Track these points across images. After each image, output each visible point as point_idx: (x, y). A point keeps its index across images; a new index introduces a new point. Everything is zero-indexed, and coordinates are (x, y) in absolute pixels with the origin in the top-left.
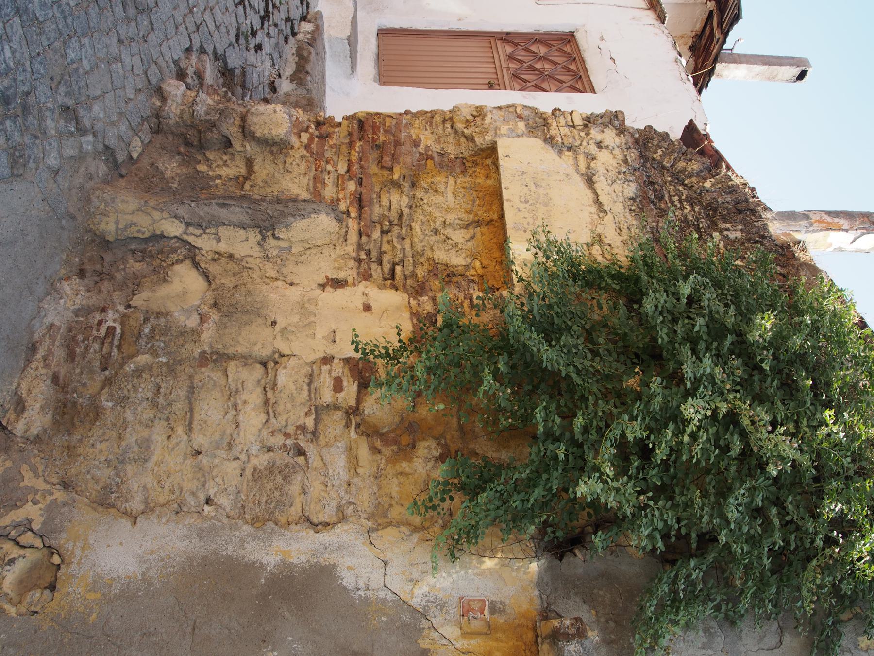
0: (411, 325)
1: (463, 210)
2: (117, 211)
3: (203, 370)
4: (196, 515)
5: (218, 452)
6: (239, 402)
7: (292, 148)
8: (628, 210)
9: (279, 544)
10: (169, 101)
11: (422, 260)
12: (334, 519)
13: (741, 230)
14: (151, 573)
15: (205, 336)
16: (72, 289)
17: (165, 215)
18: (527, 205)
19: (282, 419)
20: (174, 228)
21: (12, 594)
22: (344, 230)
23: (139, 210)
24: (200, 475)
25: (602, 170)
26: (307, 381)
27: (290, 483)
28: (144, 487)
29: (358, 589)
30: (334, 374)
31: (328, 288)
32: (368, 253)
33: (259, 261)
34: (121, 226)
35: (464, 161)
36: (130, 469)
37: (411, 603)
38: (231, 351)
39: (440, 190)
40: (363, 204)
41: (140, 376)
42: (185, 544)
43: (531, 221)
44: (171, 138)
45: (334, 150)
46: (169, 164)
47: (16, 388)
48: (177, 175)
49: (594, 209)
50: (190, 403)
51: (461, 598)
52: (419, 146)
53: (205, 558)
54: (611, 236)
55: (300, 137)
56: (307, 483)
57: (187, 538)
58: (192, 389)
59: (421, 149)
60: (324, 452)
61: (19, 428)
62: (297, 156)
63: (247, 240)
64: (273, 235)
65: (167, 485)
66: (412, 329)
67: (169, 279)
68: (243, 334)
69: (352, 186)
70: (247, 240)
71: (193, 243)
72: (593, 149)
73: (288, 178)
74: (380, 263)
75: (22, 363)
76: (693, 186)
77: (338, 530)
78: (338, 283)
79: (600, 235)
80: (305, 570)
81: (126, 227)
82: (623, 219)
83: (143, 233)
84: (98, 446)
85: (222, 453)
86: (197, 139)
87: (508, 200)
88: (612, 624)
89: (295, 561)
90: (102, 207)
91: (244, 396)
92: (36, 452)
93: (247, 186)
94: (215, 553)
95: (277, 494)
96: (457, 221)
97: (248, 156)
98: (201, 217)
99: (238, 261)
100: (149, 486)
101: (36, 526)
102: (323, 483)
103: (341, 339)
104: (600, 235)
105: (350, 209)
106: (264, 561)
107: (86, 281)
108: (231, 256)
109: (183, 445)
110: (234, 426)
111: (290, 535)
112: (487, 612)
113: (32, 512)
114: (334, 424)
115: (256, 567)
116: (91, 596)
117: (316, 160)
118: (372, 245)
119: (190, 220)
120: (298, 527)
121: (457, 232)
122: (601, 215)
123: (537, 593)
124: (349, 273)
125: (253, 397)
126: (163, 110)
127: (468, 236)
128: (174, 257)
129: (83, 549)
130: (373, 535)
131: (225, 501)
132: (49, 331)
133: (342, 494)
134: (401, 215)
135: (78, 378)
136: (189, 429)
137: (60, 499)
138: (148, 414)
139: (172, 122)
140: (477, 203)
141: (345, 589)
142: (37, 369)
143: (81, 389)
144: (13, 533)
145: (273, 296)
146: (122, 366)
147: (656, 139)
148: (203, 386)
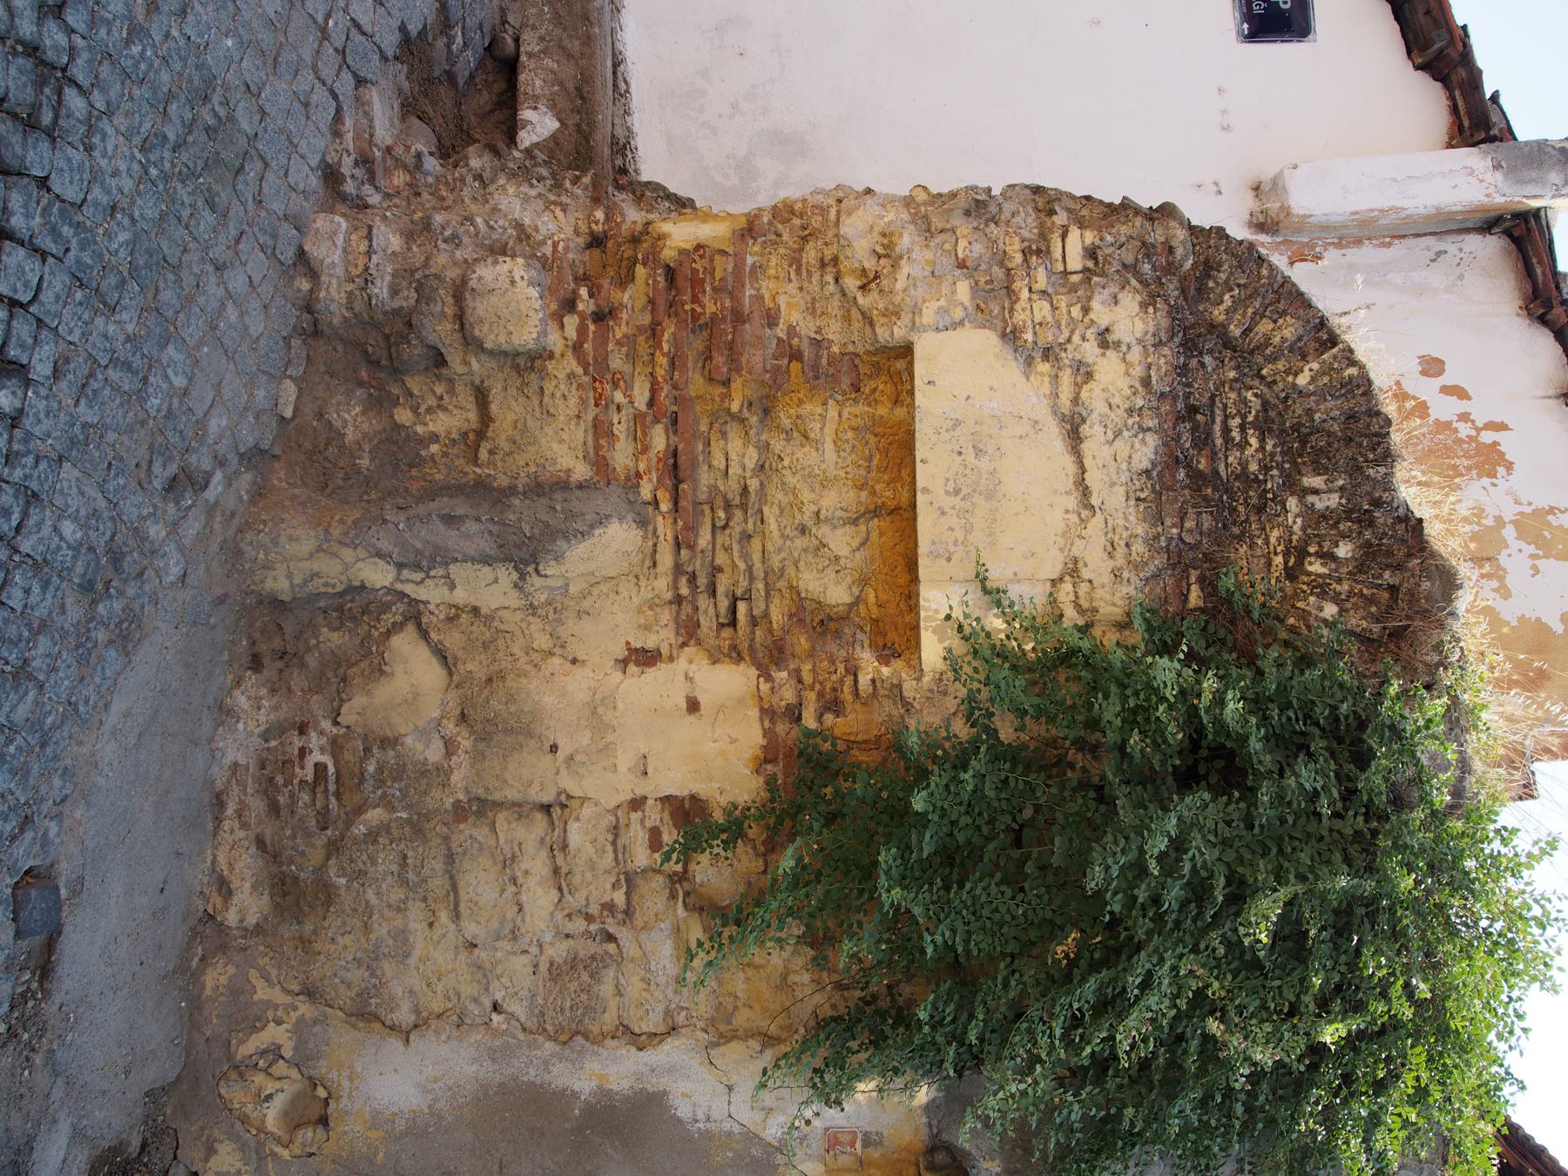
0: (760, 732)
1: (850, 483)
2: (285, 559)
3: (462, 826)
4: (482, 1028)
5: (500, 944)
6: (518, 874)
7: (551, 356)
8: (1132, 502)
9: (593, 1065)
10: (324, 278)
11: (782, 584)
12: (662, 1029)
13: (1342, 489)
14: (439, 1105)
15: (457, 778)
16: (249, 698)
17: (361, 553)
18: (956, 501)
19: (580, 897)
20: (379, 575)
21: (279, 1133)
22: (651, 543)
23: (319, 549)
24: (479, 976)
25: (1099, 406)
26: (610, 838)
27: (599, 981)
28: (411, 992)
29: (696, 1121)
30: (649, 824)
31: (632, 668)
32: (693, 578)
33: (519, 615)
34: (297, 581)
35: (857, 361)
36: (388, 968)
37: (762, 1135)
38: (497, 796)
39: (812, 435)
40: (681, 474)
41: (375, 842)
42: (474, 1068)
43: (959, 534)
44: (340, 348)
45: (624, 349)
46: (349, 412)
47: (213, 863)
48: (365, 435)
49: (1072, 502)
50: (452, 877)
51: (827, 1129)
52: (777, 325)
53: (501, 1085)
54: (1097, 565)
55: (562, 326)
56: (623, 981)
57: (476, 1060)
58: (450, 857)
59: (781, 331)
60: (643, 937)
61: (232, 918)
62: (562, 376)
63: (496, 581)
64: (536, 570)
65: (440, 988)
66: (762, 742)
67: (386, 668)
68: (511, 766)
69: (659, 439)
70: (496, 581)
71: (413, 596)
72: (1090, 350)
73: (549, 430)
74: (713, 593)
75: (210, 826)
76: (1275, 382)
77: (670, 1044)
78: (645, 658)
79: (1076, 561)
80: (627, 1099)
81: (305, 582)
82: (1121, 522)
83: (334, 586)
84: (340, 940)
85: (505, 945)
86: (385, 353)
87: (925, 490)
88: (1019, 1151)
89: (615, 1087)
90: (261, 556)
91: (525, 865)
92: (262, 948)
93: (483, 455)
94: (515, 1079)
95: (584, 997)
96: (839, 513)
97: (477, 382)
98: (418, 552)
99: (489, 619)
100: (416, 989)
101: (287, 1053)
102: (642, 980)
103: (656, 769)
104: (1076, 561)
105: (660, 495)
106: (576, 1088)
107: (266, 673)
108: (475, 611)
109: (451, 936)
110: (516, 909)
111: (605, 1053)
112: (858, 1145)
113: (275, 1034)
114: (653, 897)
115: (564, 1097)
116: (373, 1134)
117: (595, 380)
118: (698, 563)
119: (401, 559)
120: (614, 1043)
121: (839, 532)
122: (1085, 513)
123: (924, 1120)
124: (662, 637)
125: (536, 865)
126: (317, 300)
127: (856, 543)
128: (389, 619)
129: (351, 1079)
130: (712, 1052)
131: (516, 1008)
132: (234, 774)
133: (671, 995)
134: (745, 490)
135: (290, 843)
136: (457, 916)
137: (308, 1015)
138: (397, 894)
139: (336, 321)
140: (875, 462)
141: (679, 1120)
142: (232, 831)
143: (298, 859)
144: (261, 1063)
145: (549, 700)
146: (349, 824)
147: (1226, 267)
148: (464, 853)
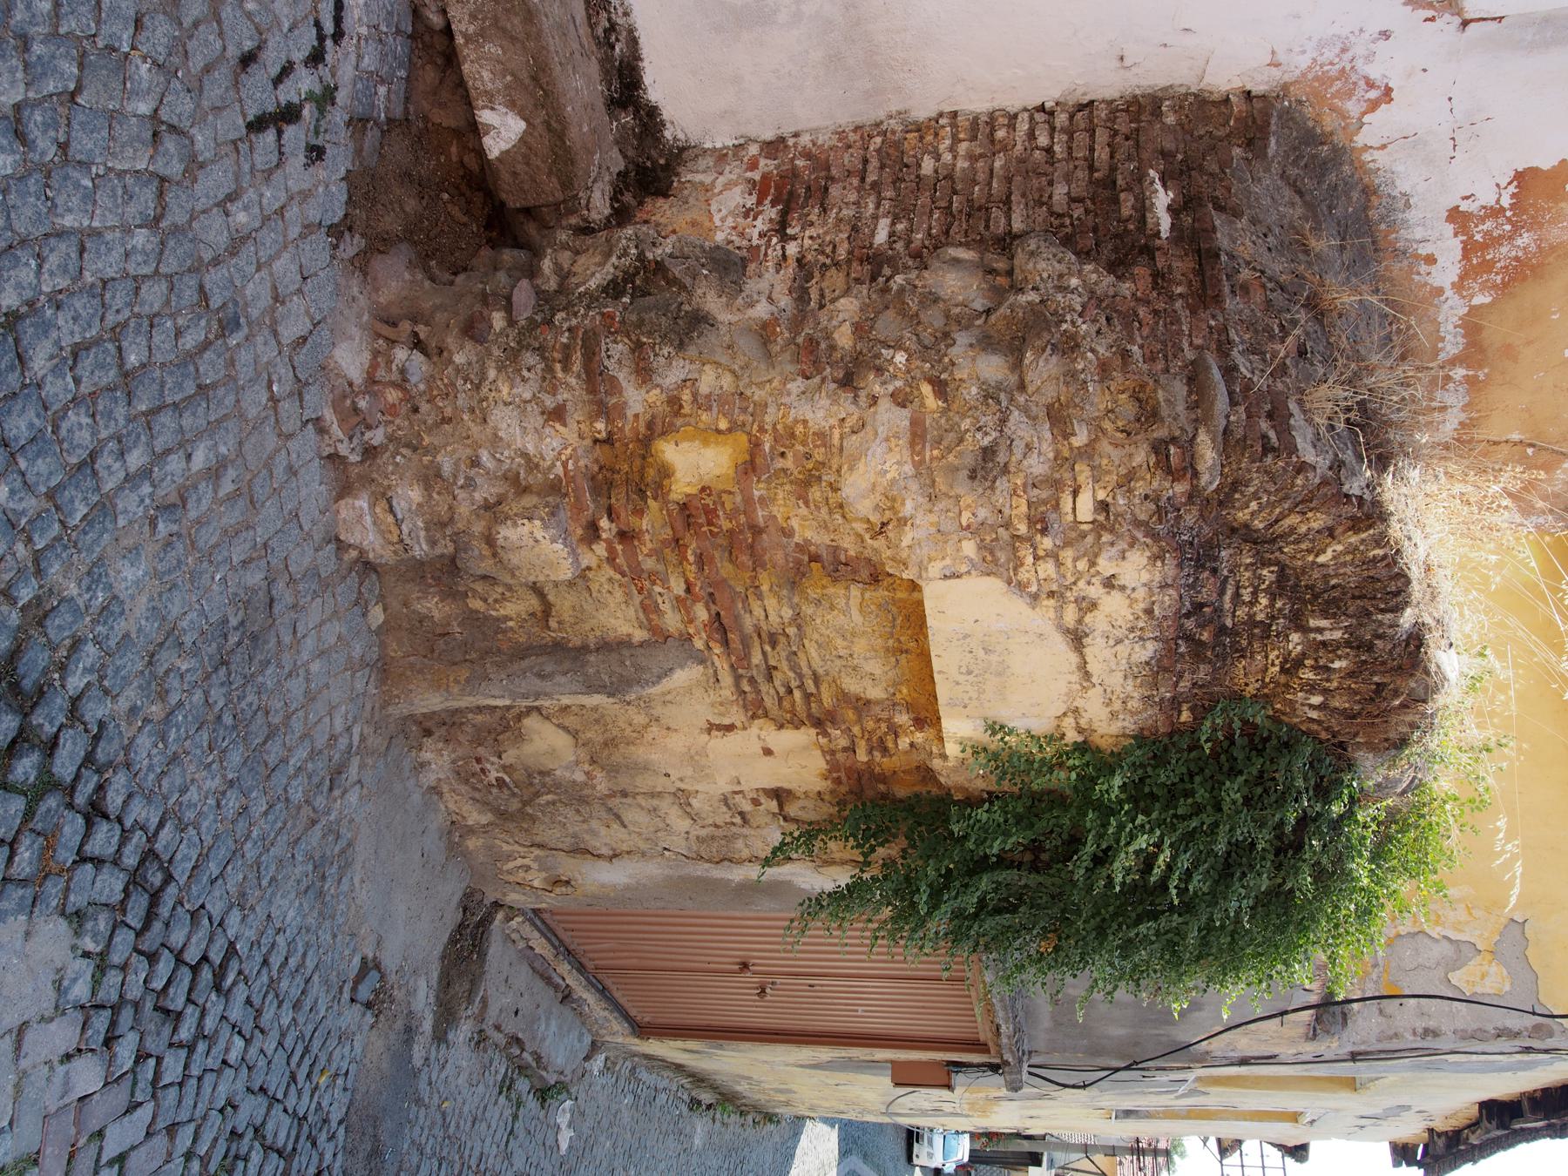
18: (970, 678)
49: (1075, 677)
62: (603, 580)
93: (553, 624)
